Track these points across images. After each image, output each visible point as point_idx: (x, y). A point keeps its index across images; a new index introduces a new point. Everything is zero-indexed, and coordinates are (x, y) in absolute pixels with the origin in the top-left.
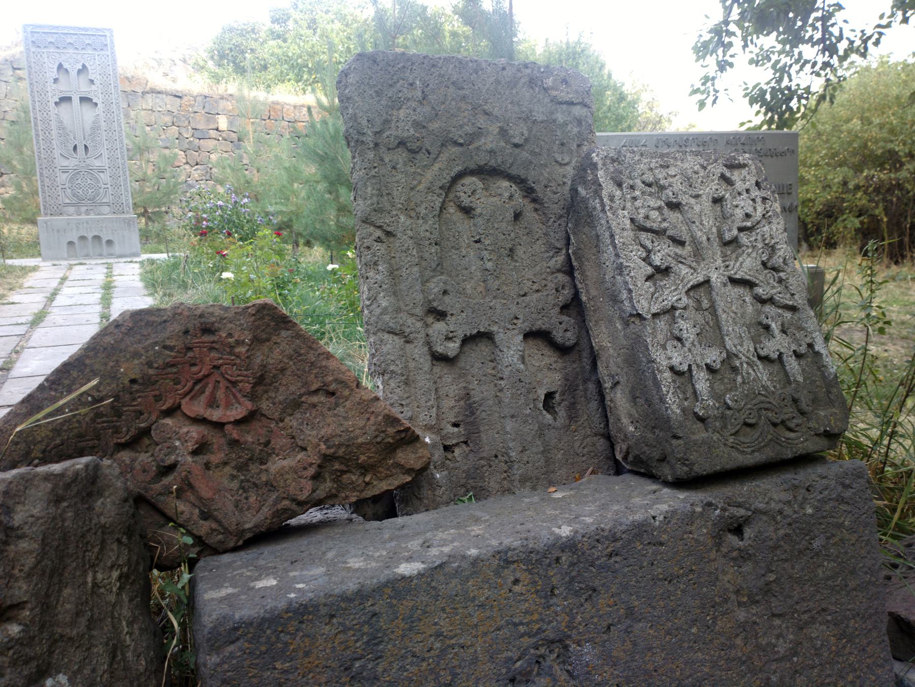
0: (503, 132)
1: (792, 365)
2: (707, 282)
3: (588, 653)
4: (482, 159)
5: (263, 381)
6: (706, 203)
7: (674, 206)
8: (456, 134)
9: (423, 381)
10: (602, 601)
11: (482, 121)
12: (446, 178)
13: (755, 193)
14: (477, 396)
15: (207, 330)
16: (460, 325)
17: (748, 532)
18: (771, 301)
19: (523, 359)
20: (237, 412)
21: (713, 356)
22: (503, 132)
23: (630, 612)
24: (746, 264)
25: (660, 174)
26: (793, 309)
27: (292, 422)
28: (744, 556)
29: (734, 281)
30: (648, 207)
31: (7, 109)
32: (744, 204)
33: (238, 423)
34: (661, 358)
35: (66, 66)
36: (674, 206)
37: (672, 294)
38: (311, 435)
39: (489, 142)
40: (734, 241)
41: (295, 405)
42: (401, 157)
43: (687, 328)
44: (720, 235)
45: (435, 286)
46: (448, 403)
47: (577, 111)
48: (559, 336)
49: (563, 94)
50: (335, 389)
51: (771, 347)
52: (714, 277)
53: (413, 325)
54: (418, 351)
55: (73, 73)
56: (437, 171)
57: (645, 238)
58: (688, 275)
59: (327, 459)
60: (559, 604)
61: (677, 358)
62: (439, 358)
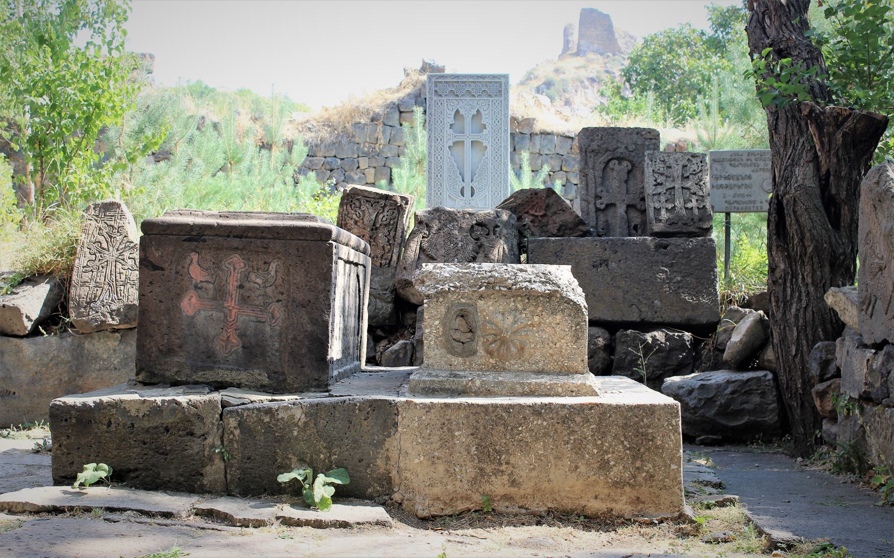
0: (626, 148)
1: (696, 211)
2: (674, 188)
3: (613, 265)
4: (618, 155)
5: (548, 207)
6: (680, 167)
7: (670, 167)
8: (610, 148)
9: (593, 214)
10: (619, 254)
11: (619, 145)
12: (606, 160)
13: (700, 164)
14: (610, 222)
15: (536, 194)
16: (605, 200)
17: (669, 248)
18: (695, 194)
19: (626, 212)
20: (541, 214)
21: (670, 206)
22: (626, 148)
23: (626, 258)
24: (689, 184)
25: (666, 159)
26: (703, 196)
27: (554, 217)
28: (665, 254)
29: (683, 188)
30: (660, 167)
31: (389, 155)
32: (695, 167)
33: (541, 216)
34: (652, 205)
35: (462, 112)
36: (670, 167)
37: (660, 189)
38: (558, 220)
39: (620, 150)
40: (688, 177)
41: (555, 213)
42: (592, 155)
43: (663, 199)
44: (683, 175)
45: (599, 190)
46: (600, 223)
47: (653, 141)
48: (639, 207)
49: (649, 136)
50: (564, 209)
51: (689, 205)
52: (677, 186)
53: (592, 200)
54: (592, 206)
55: (468, 120)
56: (603, 158)
57: (656, 175)
58: (668, 185)
59: (561, 226)
60: (607, 252)
61: (657, 205)
62: (598, 210)
